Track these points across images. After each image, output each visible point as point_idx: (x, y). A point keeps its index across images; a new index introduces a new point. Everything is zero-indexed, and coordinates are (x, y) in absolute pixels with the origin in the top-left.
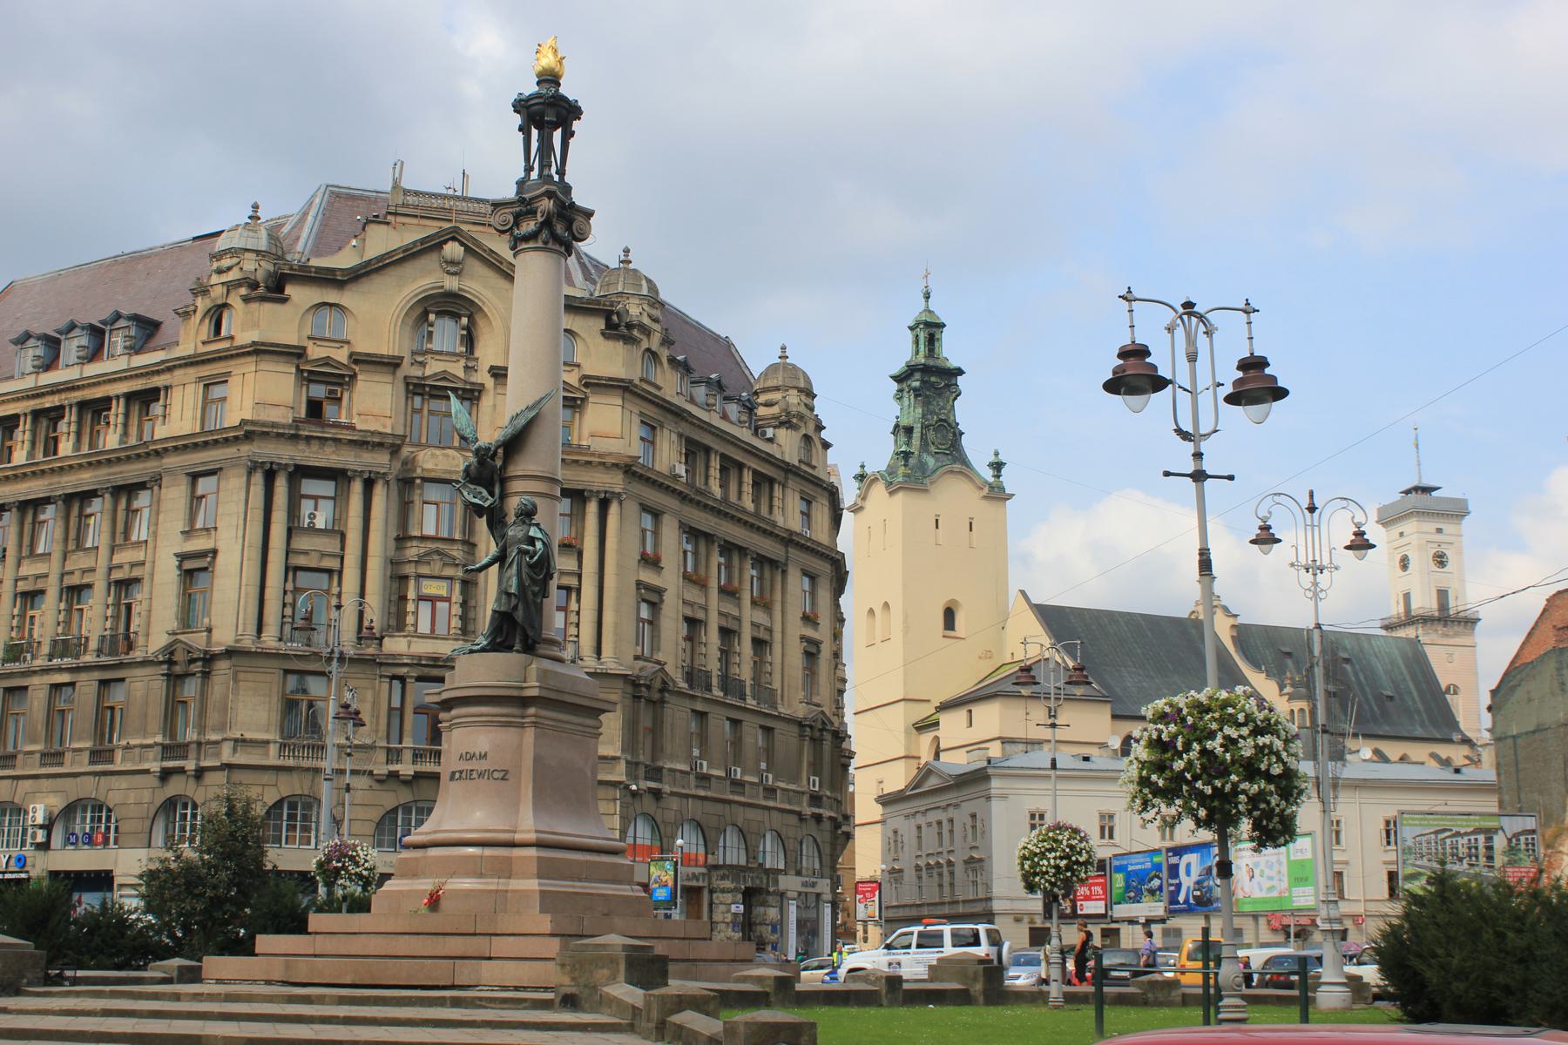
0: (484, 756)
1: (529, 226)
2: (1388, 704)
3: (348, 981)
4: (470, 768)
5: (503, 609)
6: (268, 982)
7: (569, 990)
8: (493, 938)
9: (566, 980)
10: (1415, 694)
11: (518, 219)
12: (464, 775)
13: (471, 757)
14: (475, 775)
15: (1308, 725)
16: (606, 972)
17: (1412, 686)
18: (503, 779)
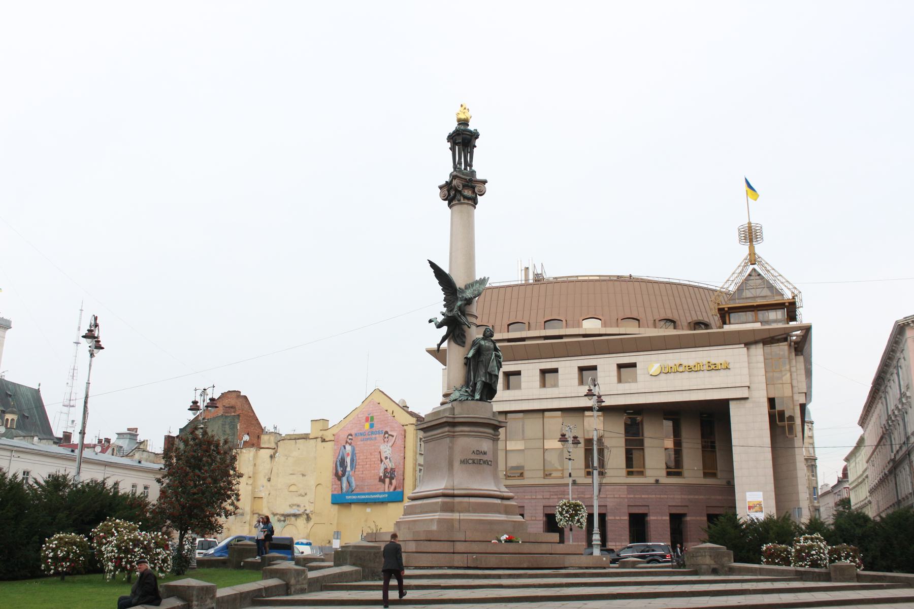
0: (485, 453)
1: (468, 193)
2: (27, 421)
3: (526, 566)
4: (479, 458)
5: (488, 381)
6: (450, 568)
7: (712, 566)
8: (553, 544)
9: (712, 562)
10: (37, 417)
11: (464, 186)
12: (476, 461)
13: (479, 452)
14: (482, 462)
15: (15, 427)
16: (727, 558)
17: (36, 413)
18: (491, 465)
